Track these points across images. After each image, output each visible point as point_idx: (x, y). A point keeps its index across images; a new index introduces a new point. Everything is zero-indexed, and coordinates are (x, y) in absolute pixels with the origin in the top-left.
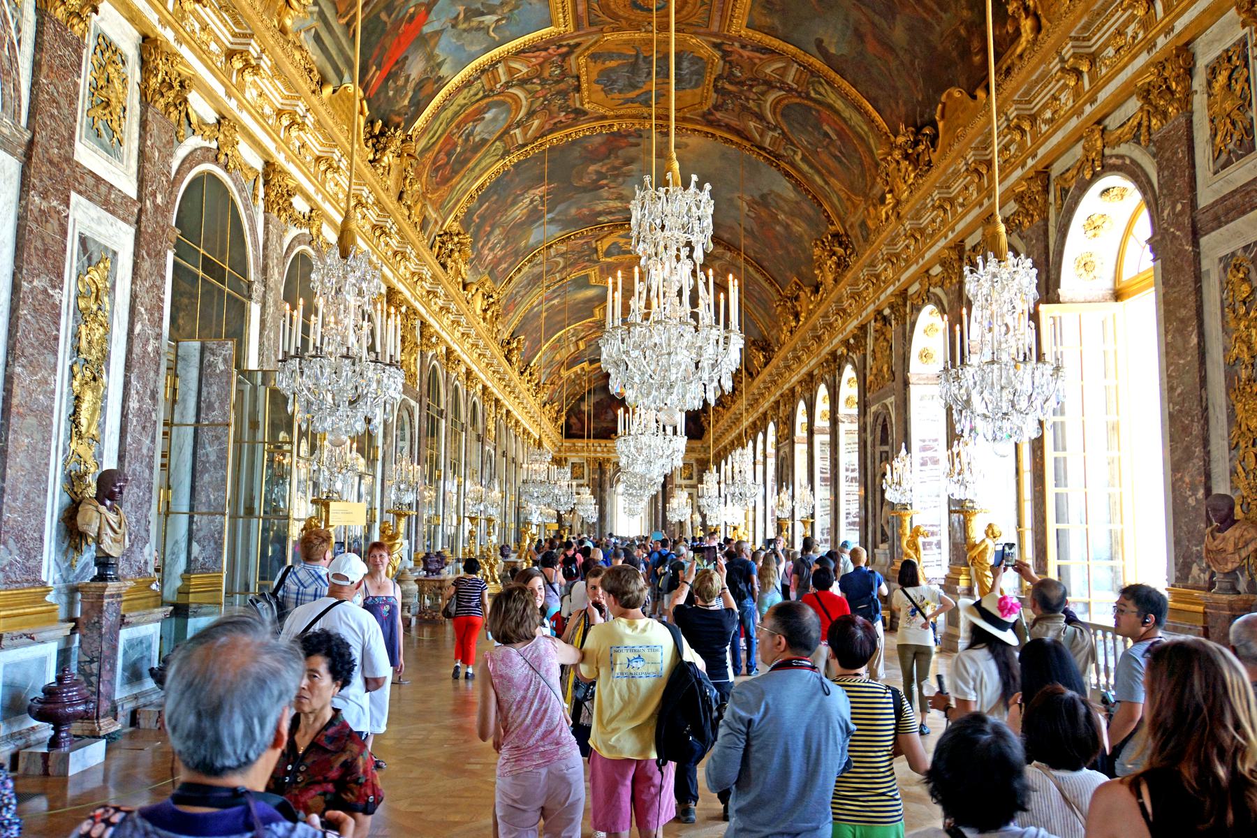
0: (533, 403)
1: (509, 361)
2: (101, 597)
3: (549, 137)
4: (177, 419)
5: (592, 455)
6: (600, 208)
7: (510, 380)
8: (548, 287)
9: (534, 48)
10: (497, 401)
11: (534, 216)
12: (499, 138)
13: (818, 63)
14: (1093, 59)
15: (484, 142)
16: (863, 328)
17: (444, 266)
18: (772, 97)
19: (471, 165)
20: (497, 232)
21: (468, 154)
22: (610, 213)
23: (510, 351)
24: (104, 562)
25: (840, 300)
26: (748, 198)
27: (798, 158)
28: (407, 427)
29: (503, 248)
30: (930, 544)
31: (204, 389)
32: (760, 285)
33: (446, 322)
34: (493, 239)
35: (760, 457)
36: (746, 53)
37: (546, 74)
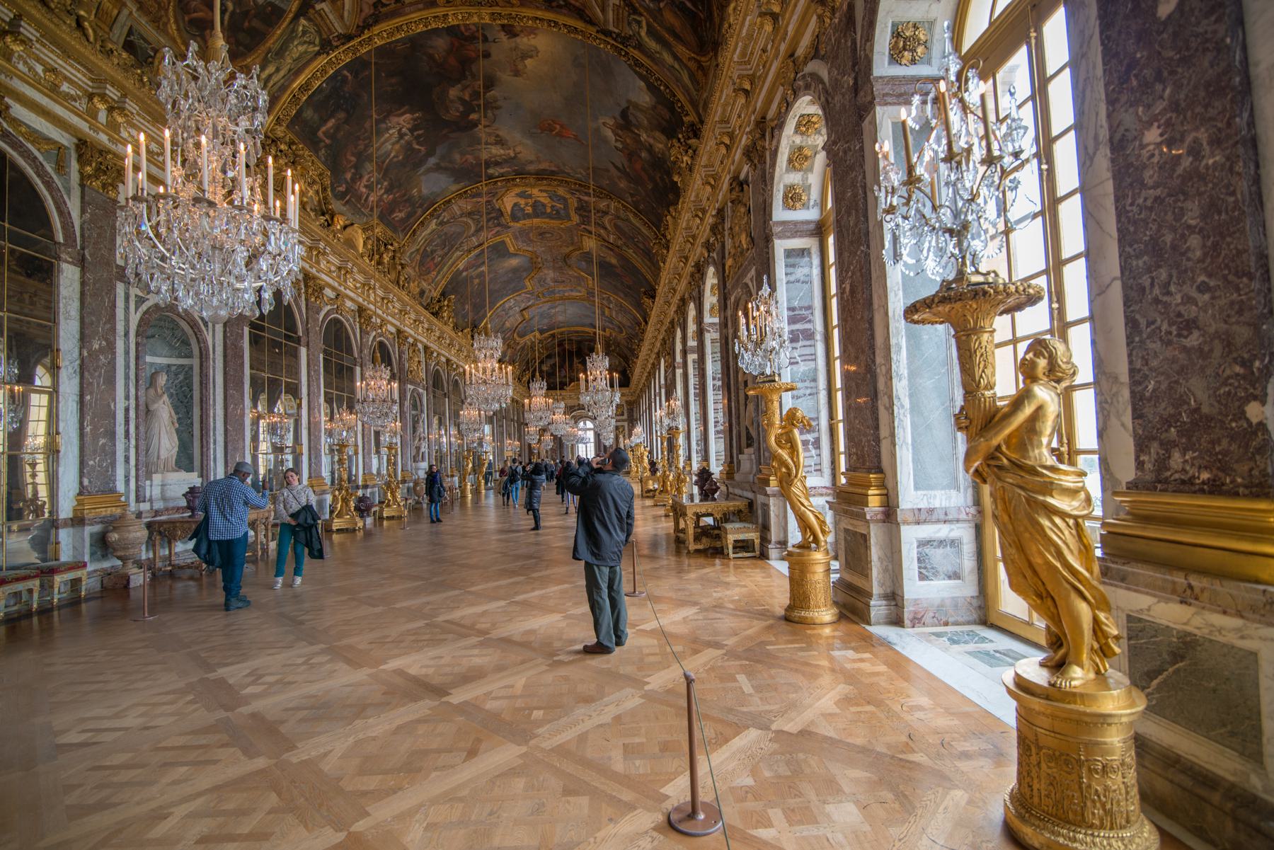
3: (376, 30)
6: (484, 156)
7: (442, 332)
8: (469, 251)
10: (426, 348)
16: (720, 212)
19: (272, 42)
20: (369, 166)
21: (256, 23)
22: (497, 164)
23: (440, 308)
25: (698, 200)
26: (611, 122)
28: (193, 341)
29: (388, 191)
32: (640, 233)
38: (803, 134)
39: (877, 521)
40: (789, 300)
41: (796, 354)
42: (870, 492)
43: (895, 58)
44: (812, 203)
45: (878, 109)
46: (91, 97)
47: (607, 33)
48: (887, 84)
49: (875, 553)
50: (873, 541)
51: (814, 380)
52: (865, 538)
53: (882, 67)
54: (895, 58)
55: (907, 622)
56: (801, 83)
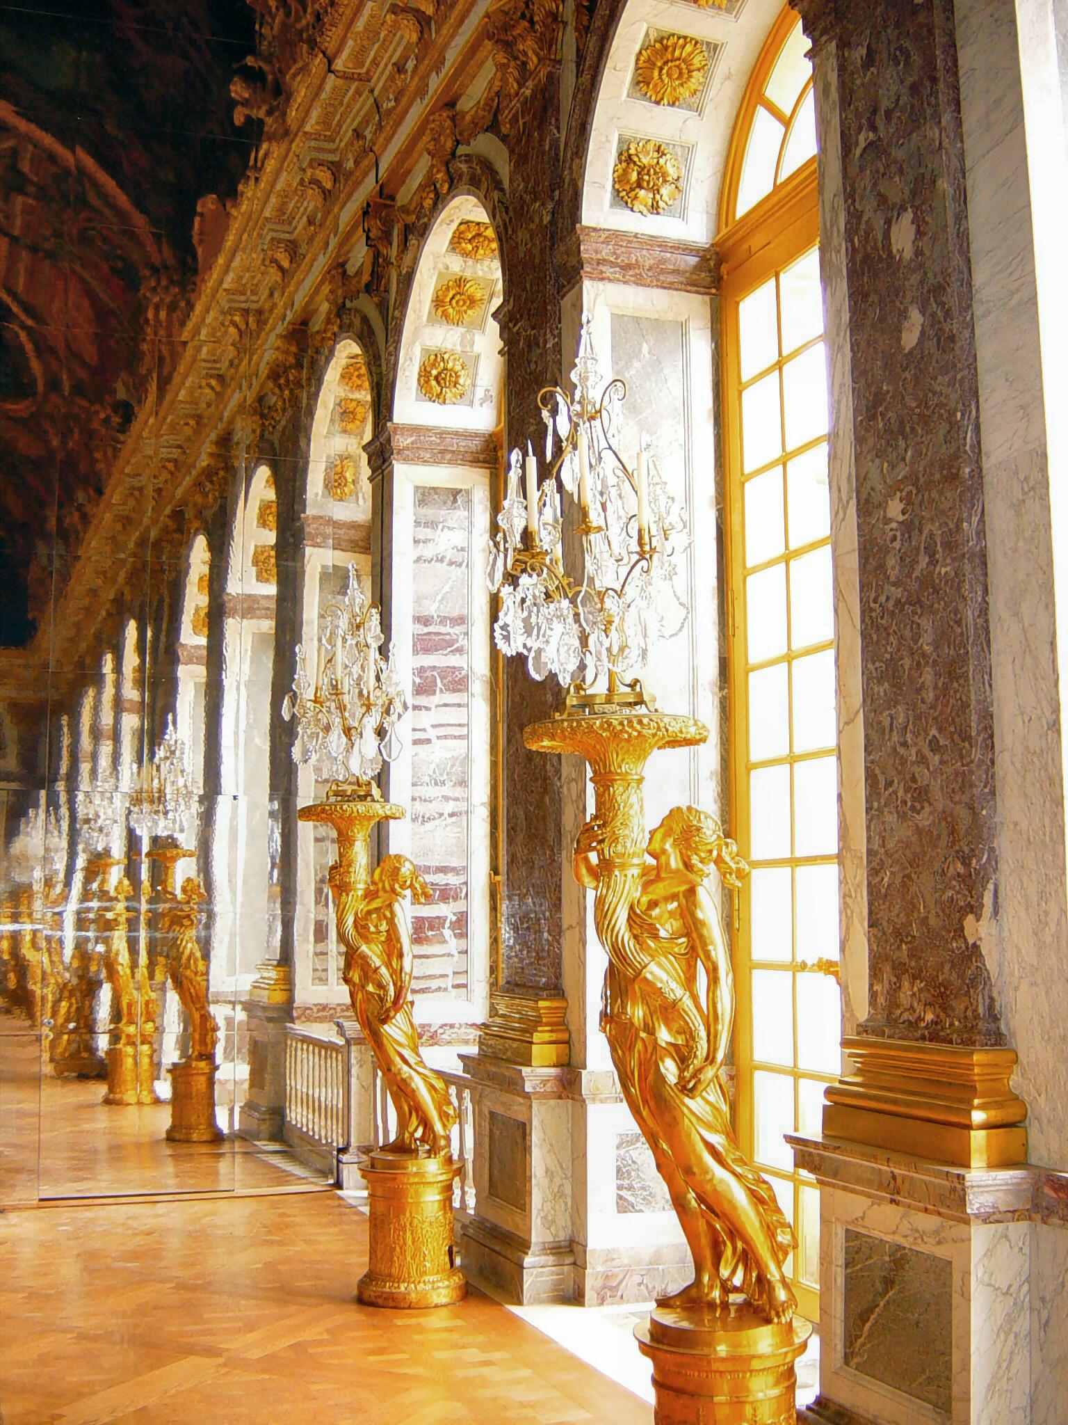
30: (437, 923)
38: (466, 254)
39: (544, 1096)
40: (418, 600)
41: (425, 719)
42: (537, 1037)
43: (624, 193)
44: (480, 393)
45: (587, 285)
48: (606, 242)
49: (539, 1160)
50: (536, 1137)
51: (463, 783)
52: (523, 1129)
53: (598, 209)
54: (624, 193)
55: (589, 1294)
56: (464, 167)
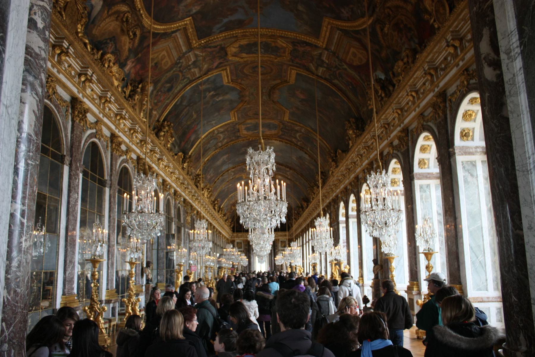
0: (222, 222)
1: (214, 209)
2: (149, 287)
4: (153, 248)
5: (245, 239)
9: (226, 125)
11: (224, 163)
12: (214, 146)
13: (310, 129)
14: (361, 155)
15: (209, 148)
16: (330, 203)
17: (197, 186)
18: (298, 135)
20: (212, 170)
23: (215, 205)
24: (148, 281)
27: (308, 149)
31: (159, 241)
33: (197, 203)
34: (210, 172)
35: (307, 240)
36: (289, 124)
37: (229, 130)
46: (185, 188)
47: (297, 145)
